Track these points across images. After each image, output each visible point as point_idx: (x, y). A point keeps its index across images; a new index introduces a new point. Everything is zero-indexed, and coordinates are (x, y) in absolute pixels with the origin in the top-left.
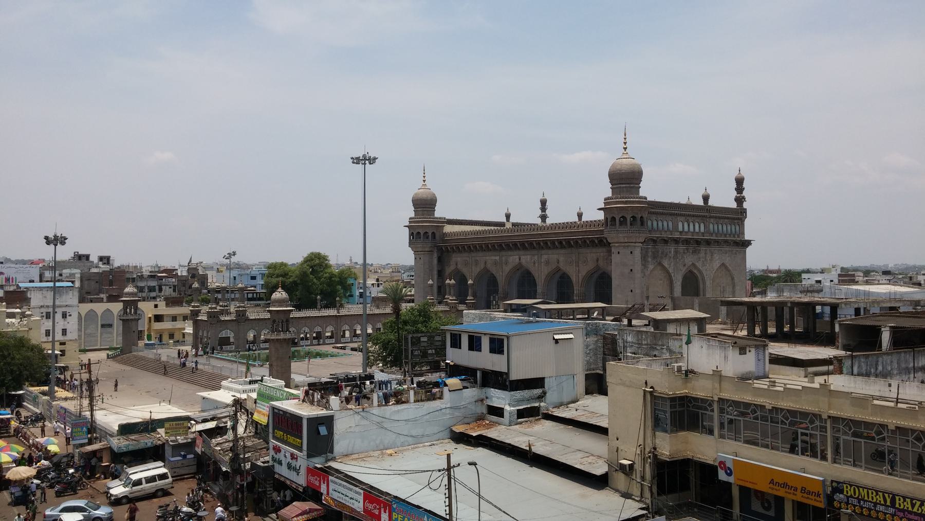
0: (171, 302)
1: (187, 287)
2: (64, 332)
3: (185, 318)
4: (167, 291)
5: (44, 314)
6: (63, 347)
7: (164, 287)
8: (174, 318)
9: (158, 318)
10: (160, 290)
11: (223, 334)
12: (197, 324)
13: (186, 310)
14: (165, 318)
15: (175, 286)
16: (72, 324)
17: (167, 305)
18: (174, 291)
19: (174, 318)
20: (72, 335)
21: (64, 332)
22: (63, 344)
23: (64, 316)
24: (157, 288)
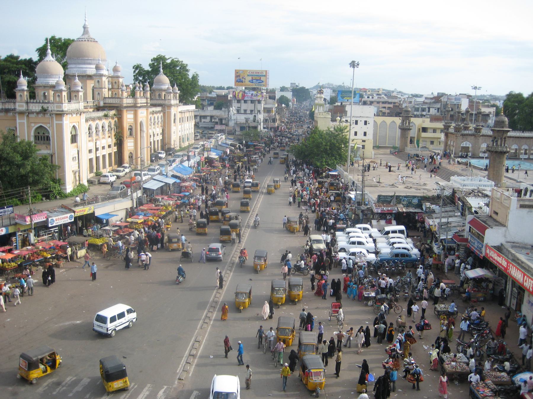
0: (434, 119)
1: (445, 110)
2: (365, 134)
3: (442, 131)
4: (433, 111)
5: (354, 122)
6: (364, 143)
7: (431, 109)
8: (434, 131)
9: (425, 130)
10: (429, 111)
11: (464, 144)
12: (447, 135)
13: (440, 125)
14: (429, 130)
15: (438, 109)
16: (370, 129)
17: (431, 121)
18: (438, 111)
19: (434, 131)
20: (370, 137)
21: (365, 134)
22: (364, 141)
23: (366, 123)
24: (427, 109)
